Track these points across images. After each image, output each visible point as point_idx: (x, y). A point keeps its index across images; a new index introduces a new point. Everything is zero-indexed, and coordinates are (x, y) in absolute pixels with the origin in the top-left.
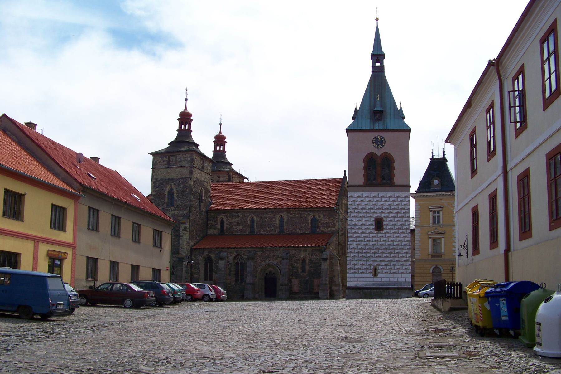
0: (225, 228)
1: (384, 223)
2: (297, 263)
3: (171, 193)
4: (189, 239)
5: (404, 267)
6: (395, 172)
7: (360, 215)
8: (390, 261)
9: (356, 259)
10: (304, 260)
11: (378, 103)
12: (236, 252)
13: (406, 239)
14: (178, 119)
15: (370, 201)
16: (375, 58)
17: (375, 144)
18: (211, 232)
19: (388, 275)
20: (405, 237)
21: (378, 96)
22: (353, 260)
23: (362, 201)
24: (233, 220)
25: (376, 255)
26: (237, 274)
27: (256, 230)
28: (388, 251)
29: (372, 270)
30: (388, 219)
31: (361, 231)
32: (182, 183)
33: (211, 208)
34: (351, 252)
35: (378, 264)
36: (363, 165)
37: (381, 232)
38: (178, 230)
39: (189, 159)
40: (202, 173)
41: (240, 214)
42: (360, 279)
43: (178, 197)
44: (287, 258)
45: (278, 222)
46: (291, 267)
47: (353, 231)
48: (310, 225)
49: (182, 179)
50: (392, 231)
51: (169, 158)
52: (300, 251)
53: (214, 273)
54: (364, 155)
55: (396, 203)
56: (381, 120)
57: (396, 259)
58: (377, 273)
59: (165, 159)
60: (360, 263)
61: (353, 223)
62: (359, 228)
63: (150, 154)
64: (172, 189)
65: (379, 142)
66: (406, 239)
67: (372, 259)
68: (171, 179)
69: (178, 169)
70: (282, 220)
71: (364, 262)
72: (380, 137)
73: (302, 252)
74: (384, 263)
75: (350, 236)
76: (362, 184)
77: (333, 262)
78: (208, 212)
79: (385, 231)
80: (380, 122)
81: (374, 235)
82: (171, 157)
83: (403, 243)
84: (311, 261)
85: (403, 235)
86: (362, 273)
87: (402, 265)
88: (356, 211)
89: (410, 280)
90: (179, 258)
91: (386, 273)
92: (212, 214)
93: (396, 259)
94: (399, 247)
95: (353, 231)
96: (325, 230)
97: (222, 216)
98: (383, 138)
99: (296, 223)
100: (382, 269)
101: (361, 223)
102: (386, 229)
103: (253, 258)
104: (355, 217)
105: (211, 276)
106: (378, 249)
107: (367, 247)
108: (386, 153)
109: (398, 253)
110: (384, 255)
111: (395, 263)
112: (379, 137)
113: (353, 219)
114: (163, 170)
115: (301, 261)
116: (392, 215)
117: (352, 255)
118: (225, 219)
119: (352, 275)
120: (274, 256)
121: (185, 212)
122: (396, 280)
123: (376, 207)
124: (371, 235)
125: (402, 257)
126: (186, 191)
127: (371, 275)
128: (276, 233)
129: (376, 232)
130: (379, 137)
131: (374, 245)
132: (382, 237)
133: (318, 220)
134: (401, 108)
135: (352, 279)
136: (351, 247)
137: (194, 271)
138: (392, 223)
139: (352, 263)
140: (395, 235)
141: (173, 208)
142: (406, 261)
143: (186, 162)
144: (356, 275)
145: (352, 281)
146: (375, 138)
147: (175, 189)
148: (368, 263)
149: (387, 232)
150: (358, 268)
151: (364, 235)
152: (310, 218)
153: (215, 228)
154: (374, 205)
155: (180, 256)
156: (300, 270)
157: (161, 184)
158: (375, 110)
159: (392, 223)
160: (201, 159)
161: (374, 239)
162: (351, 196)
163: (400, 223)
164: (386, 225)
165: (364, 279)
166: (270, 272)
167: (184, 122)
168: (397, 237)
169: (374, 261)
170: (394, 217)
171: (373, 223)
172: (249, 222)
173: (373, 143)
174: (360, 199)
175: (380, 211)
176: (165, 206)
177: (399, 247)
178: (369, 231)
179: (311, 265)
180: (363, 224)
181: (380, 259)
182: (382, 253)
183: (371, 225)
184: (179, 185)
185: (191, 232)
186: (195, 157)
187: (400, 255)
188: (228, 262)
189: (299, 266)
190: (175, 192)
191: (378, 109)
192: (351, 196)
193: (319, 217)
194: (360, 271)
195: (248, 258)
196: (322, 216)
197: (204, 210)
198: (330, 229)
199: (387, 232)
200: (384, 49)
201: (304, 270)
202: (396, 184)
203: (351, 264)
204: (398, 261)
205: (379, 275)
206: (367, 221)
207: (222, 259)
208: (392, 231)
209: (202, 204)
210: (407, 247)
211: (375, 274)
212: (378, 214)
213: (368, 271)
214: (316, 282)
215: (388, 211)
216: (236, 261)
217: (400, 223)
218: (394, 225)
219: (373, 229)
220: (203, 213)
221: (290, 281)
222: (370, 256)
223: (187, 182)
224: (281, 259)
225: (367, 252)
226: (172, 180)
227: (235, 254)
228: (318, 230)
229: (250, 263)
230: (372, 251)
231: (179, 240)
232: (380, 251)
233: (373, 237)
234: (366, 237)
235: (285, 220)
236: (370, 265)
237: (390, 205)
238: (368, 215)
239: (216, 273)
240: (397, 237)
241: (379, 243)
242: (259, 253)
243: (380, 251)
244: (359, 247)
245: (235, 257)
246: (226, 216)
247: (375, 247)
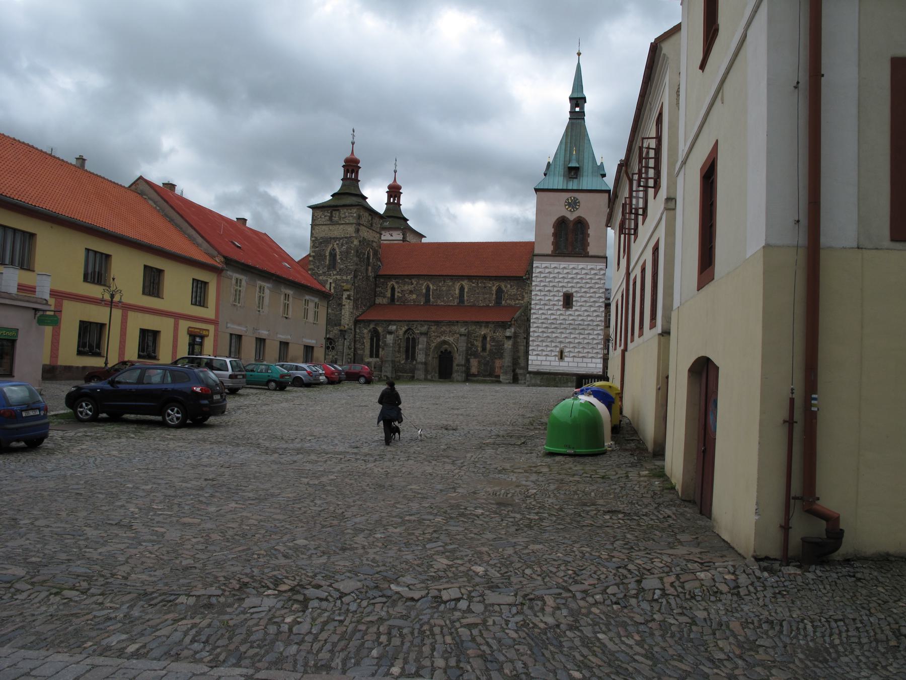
0: (396, 297)
1: (574, 299)
2: (477, 340)
3: (333, 255)
4: (353, 309)
5: (595, 351)
6: (589, 240)
7: (547, 289)
8: (579, 343)
9: (540, 339)
10: (484, 337)
11: (574, 157)
12: (407, 325)
13: (598, 319)
14: (343, 166)
15: (559, 273)
16: (575, 102)
18: (379, 300)
19: (576, 360)
20: (597, 316)
23: (550, 273)
24: (406, 288)
25: (563, 336)
26: (407, 351)
27: (432, 299)
31: (547, 307)
32: (346, 243)
33: (381, 272)
34: (534, 332)
36: (552, 230)
38: (341, 299)
39: (355, 215)
40: (371, 231)
41: (413, 281)
42: (544, 363)
43: (341, 259)
44: (465, 335)
45: (457, 292)
46: (469, 345)
47: (538, 307)
48: (494, 296)
49: (346, 238)
50: (583, 309)
51: (331, 213)
52: (481, 326)
53: (381, 349)
54: (554, 219)
55: (588, 277)
56: (576, 178)
57: (586, 341)
59: (326, 214)
60: (544, 344)
61: (538, 298)
62: (545, 304)
63: (310, 207)
64: (334, 249)
65: (573, 204)
66: (598, 319)
67: (558, 340)
68: (334, 238)
69: (342, 226)
70: (462, 289)
73: (483, 328)
74: (572, 345)
75: (534, 313)
76: (550, 253)
77: (519, 340)
78: (377, 277)
79: (574, 308)
80: (575, 181)
82: (334, 212)
83: (595, 323)
84: (493, 339)
85: (595, 314)
86: (547, 355)
87: (593, 348)
88: (542, 284)
89: (601, 366)
90: (341, 331)
92: (382, 280)
93: (586, 341)
94: (590, 328)
95: (538, 307)
96: (513, 303)
97: (393, 282)
99: (478, 294)
101: (547, 298)
102: (576, 305)
103: (426, 334)
104: (540, 290)
105: (378, 351)
106: (565, 328)
107: (553, 326)
108: (579, 217)
109: (589, 334)
113: (539, 293)
114: (324, 227)
115: (481, 339)
116: (583, 290)
117: (536, 334)
118: (396, 286)
120: (450, 331)
121: (349, 277)
122: (585, 365)
123: (566, 280)
124: (559, 313)
125: (593, 339)
126: (350, 253)
128: (456, 304)
131: (561, 324)
132: (570, 315)
133: (504, 291)
134: (602, 163)
135: (534, 363)
136: (535, 325)
137: (358, 346)
138: (583, 299)
139: (535, 343)
140: (586, 314)
141: (335, 272)
142: (597, 344)
143: (351, 218)
147: (337, 250)
148: (553, 344)
149: (576, 310)
150: (542, 350)
151: (550, 312)
152: (494, 288)
153: (384, 297)
154: (563, 278)
155: (342, 328)
156: (480, 349)
157: (321, 243)
158: (570, 165)
159: (583, 299)
160: (370, 215)
161: (562, 317)
162: (537, 267)
163: (592, 300)
164: (577, 301)
165: (548, 363)
166: (446, 350)
167: (350, 170)
168: (588, 316)
169: (561, 342)
170: (585, 292)
171: (562, 298)
172: (424, 291)
173: (566, 205)
174: (547, 270)
175: (570, 285)
176: (326, 268)
177: (590, 328)
178: (556, 308)
179: (493, 344)
180: (549, 300)
181: (567, 340)
182: (571, 333)
183: (559, 300)
184: (342, 245)
185: (356, 301)
186: (362, 212)
187: (591, 337)
188: (398, 337)
189: (479, 344)
190: (338, 253)
191: (574, 164)
192: (537, 267)
193: (506, 287)
194: (544, 353)
195: (421, 334)
196: (509, 286)
197: (371, 274)
198: (517, 302)
199: (576, 310)
200: (586, 93)
201: (484, 349)
204: (588, 343)
205: (566, 359)
206: (554, 296)
207: (390, 333)
208: (583, 309)
209: (370, 268)
211: (561, 356)
213: (553, 354)
214: (498, 363)
215: (579, 285)
216: (406, 336)
217: (592, 300)
218: (585, 301)
220: (371, 278)
221: (468, 361)
222: (556, 337)
223: (352, 242)
224: (458, 335)
225: (553, 332)
226: (335, 239)
227: (406, 328)
228: (503, 302)
229: (423, 340)
231: (341, 310)
232: (568, 331)
233: (561, 314)
234: (552, 314)
235: (466, 290)
236: (556, 346)
237: (582, 278)
239: (383, 349)
240: (588, 316)
241: (568, 322)
242: (433, 328)
243: (568, 331)
244: (544, 326)
245: (405, 332)
246: (397, 283)
247: (563, 326)
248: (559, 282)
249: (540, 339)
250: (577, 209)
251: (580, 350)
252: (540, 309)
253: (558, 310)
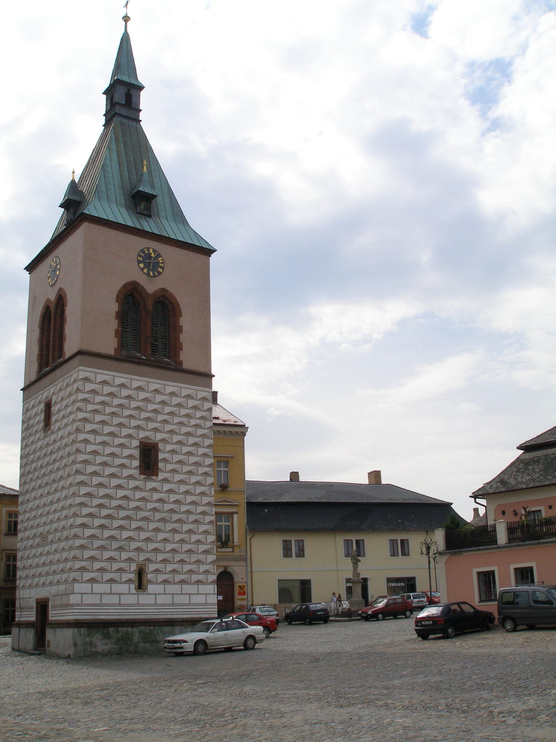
1: (161, 456)
6: (183, 338)
13: (205, 500)
17: (142, 265)
20: (203, 494)
22: (90, 546)
28: (169, 526)
29: (133, 575)
30: (169, 447)
35: (148, 560)
36: (114, 307)
37: (153, 477)
42: (106, 600)
58: (144, 581)
62: (104, 464)
66: (205, 500)
71: (96, 552)
72: (155, 251)
76: (112, 352)
79: (161, 476)
81: (137, 483)
86: (112, 581)
91: (166, 582)
98: (159, 256)
100: (157, 571)
101: (108, 450)
104: (93, 432)
106: (145, 519)
107: (122, 514)
108: (164, 290)
110: (161, 536)
111: (183, 556)
112: (151, 251)
113: (91, 437)
119: (86, 587)
125: (198, 542)
127: (133, 586)
129: (142, 477)
130: (151, 251)
131: (138, 508)
132: (154, 490)
142: (206, 552)
144: (97, 588)
145: (86, 605)
146: (143, 251)
148: (125, 556)
149: (165, 480)
150: (102, 570)
161: (139, 495)
164: (165, 460)
165: (115, 599)
171: (136, 453)
174: (107, 389)
178: (126, 472)
180: (113, 455)
181: (152, 546)
182: (157, 530)
183: (131, 457)
199: (165, 480)
203: (85, 557)
205: (151, 588)
208: (178, 477)
210: (208, 519)
211: (141, 586)
212: (147, 433)
219: (135, 468)
222: (130, 538)
225: (121, 528)
230: (134, 525)
232: (152, 526)
233: (136, 488)
236: (130, 560)
238: (125, 432)
241: (150, 506)
244: (104, 512)
247: (141, 514)
248: (131, 416)
249: (97, 543)
250: (160, 273)
251: (176, 566)
252: (95, 473)
253: (130, 477)
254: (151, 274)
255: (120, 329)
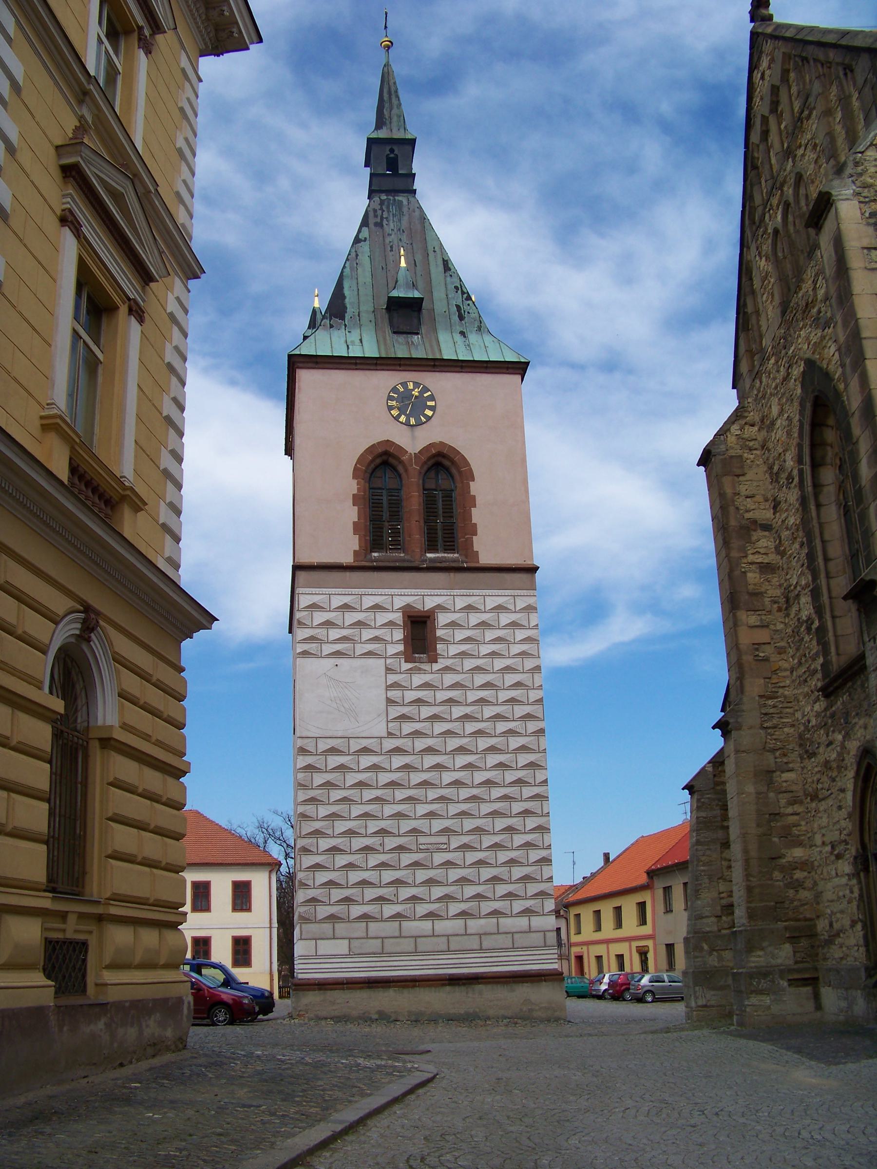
17: (395, 413)
21: (402, 252)
72: (416, 385)
146: (394, 389)
158: (395, 294)
173: (390, 408)
202: (485, 559)
254: (412, 421)
255: (362, 521)
